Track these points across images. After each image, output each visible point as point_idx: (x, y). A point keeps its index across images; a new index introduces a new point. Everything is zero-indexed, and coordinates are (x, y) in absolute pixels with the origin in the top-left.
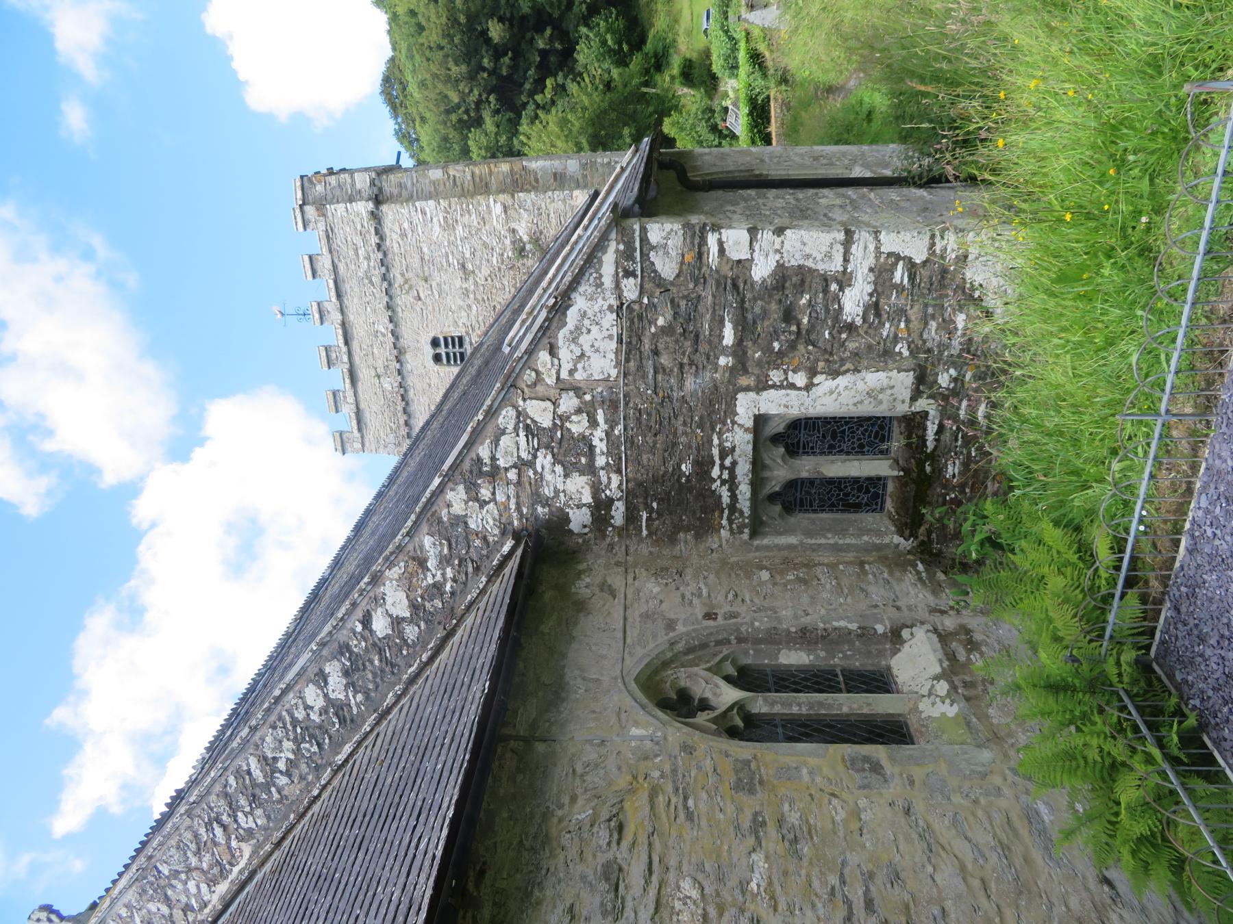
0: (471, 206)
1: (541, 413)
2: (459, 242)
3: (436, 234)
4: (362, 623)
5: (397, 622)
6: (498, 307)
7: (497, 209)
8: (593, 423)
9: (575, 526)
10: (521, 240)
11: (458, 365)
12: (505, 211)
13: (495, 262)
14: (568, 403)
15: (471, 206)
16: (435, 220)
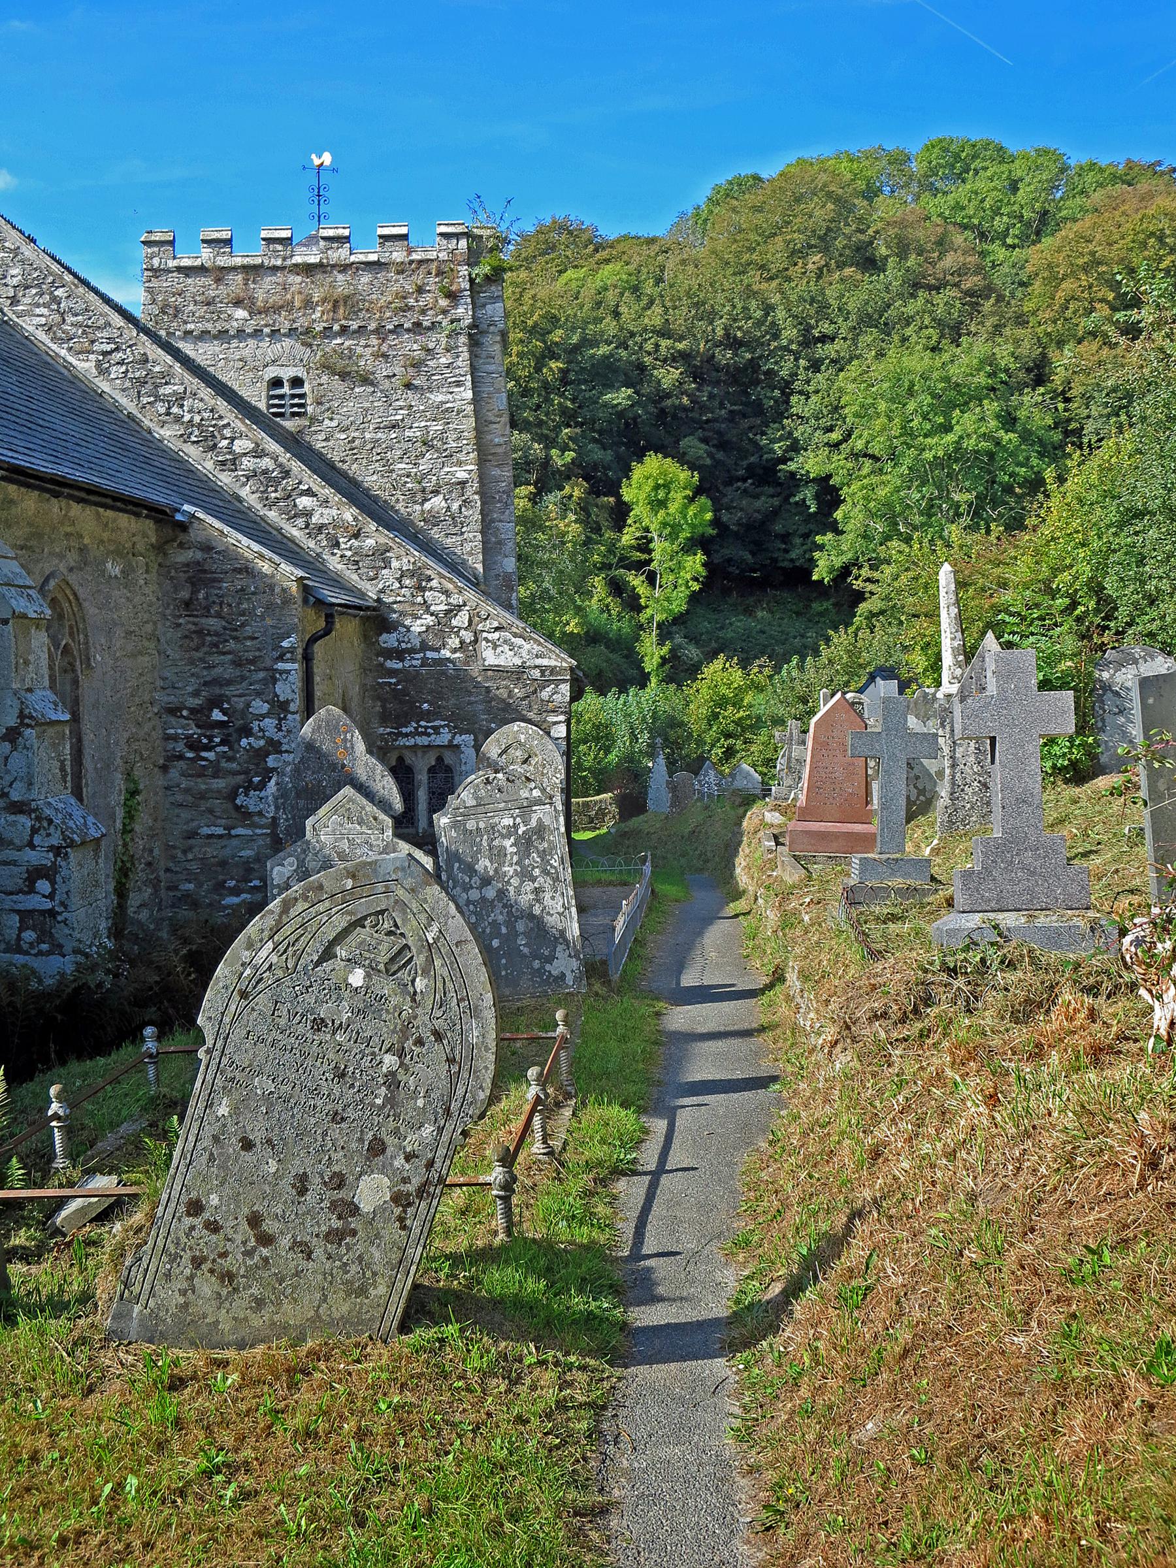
0: (465, 442)
1: (461, 620)
2: (423, 424)
3: (432, 397)
4: (309, 489)
5: (308, 514)
6: (345, 467)
7: (462, 475)
8: (454, 651)
9: (385, 636)
10: (426, 500)
11: (268, 409)
12: (459, 483)
13: (403, 466)
14: (468, 636)
15: (465, 442)
16: (450, 397)
